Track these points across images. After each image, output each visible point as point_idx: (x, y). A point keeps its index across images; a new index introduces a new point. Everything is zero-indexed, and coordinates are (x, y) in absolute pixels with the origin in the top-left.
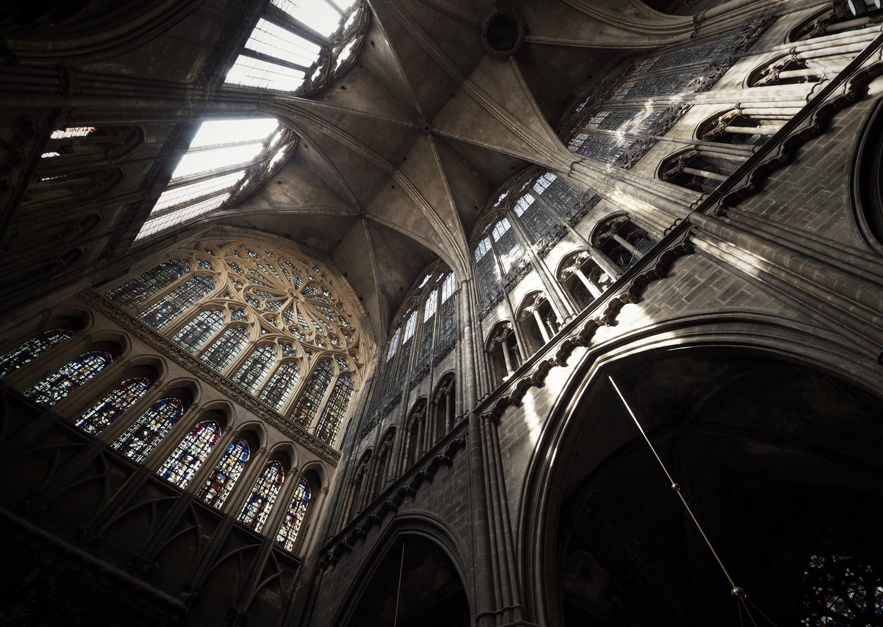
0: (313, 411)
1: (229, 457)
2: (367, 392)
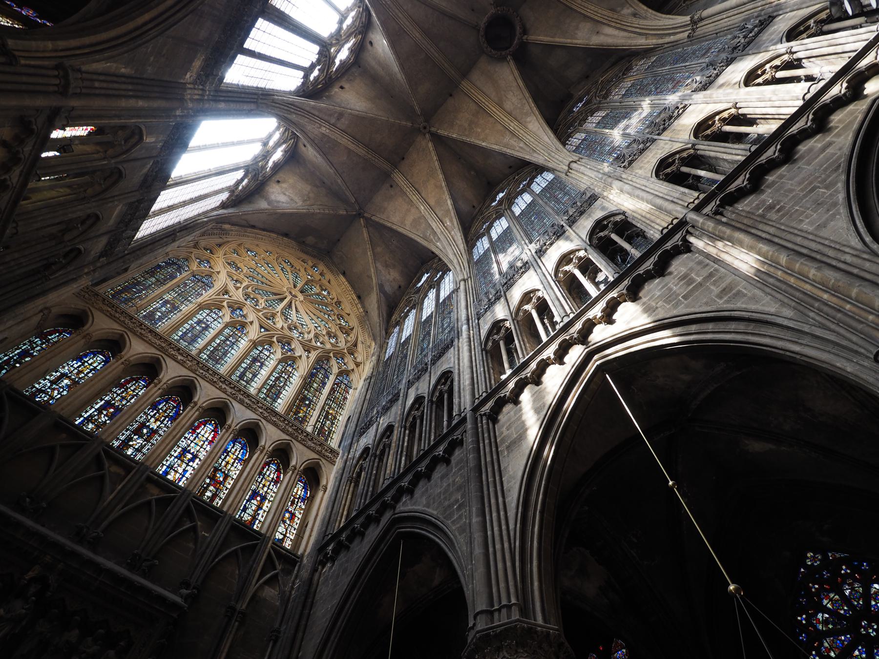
0: (312, 409)
1: (228, 455)
2: (366, 390)
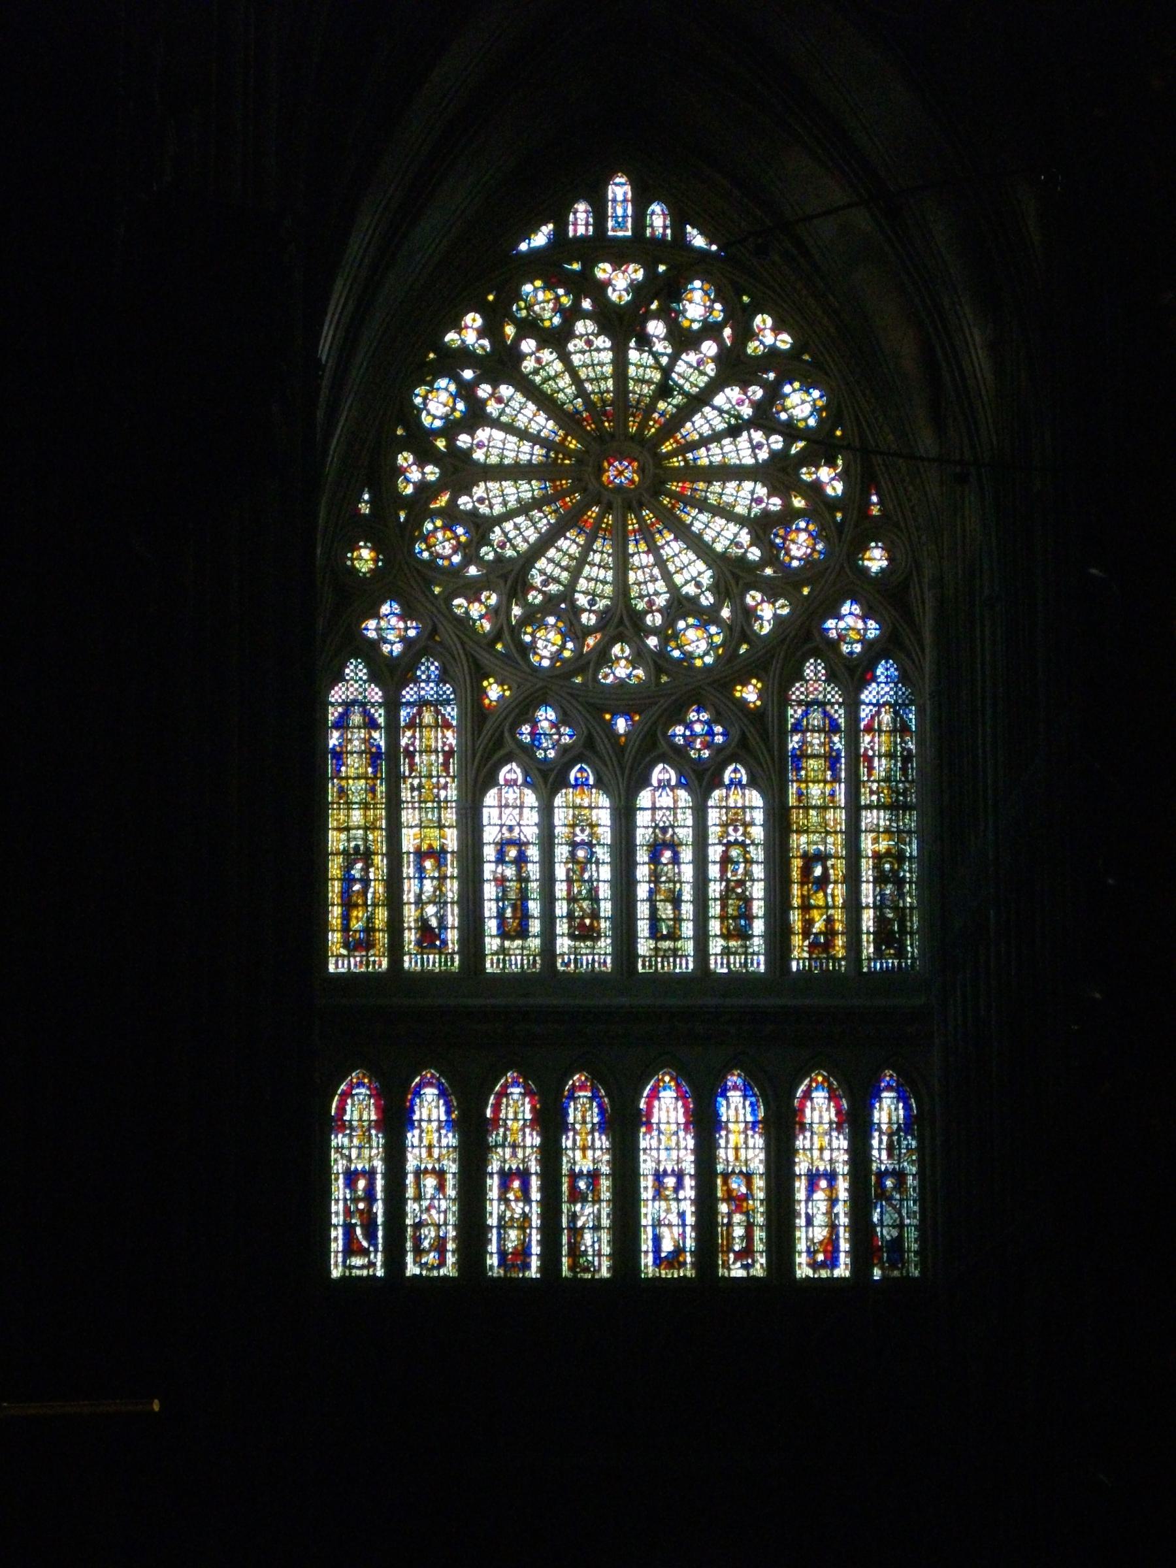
0: (836, 882)
1: (728, 1131)
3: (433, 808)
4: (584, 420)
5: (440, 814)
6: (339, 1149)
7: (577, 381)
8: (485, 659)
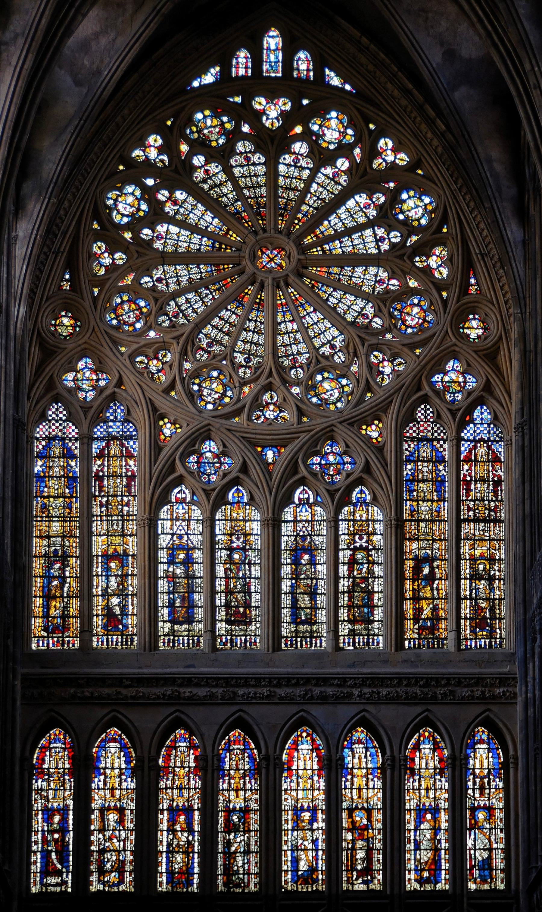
0: (440, 579)
1: (353, 776)
3: (117, 520)
4: (243, 218)
5: (123, 525)
6: (39, 791)
7: (237, 187)
8: (162, 403)
